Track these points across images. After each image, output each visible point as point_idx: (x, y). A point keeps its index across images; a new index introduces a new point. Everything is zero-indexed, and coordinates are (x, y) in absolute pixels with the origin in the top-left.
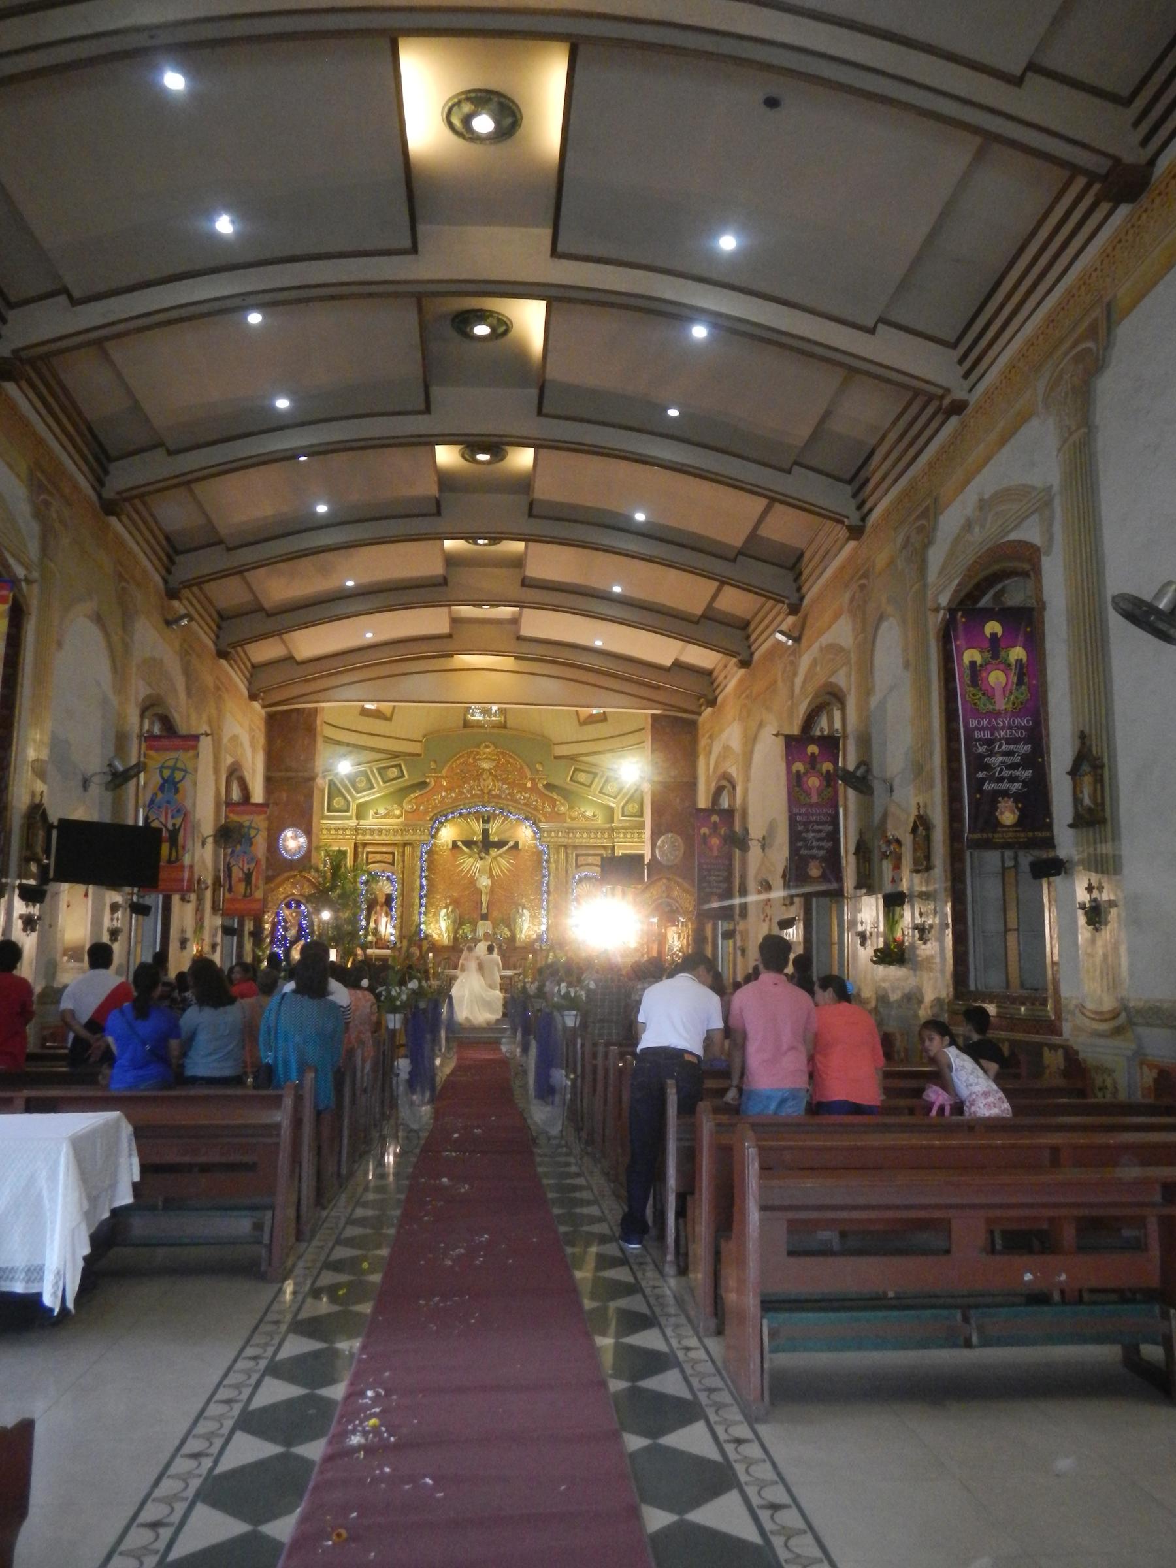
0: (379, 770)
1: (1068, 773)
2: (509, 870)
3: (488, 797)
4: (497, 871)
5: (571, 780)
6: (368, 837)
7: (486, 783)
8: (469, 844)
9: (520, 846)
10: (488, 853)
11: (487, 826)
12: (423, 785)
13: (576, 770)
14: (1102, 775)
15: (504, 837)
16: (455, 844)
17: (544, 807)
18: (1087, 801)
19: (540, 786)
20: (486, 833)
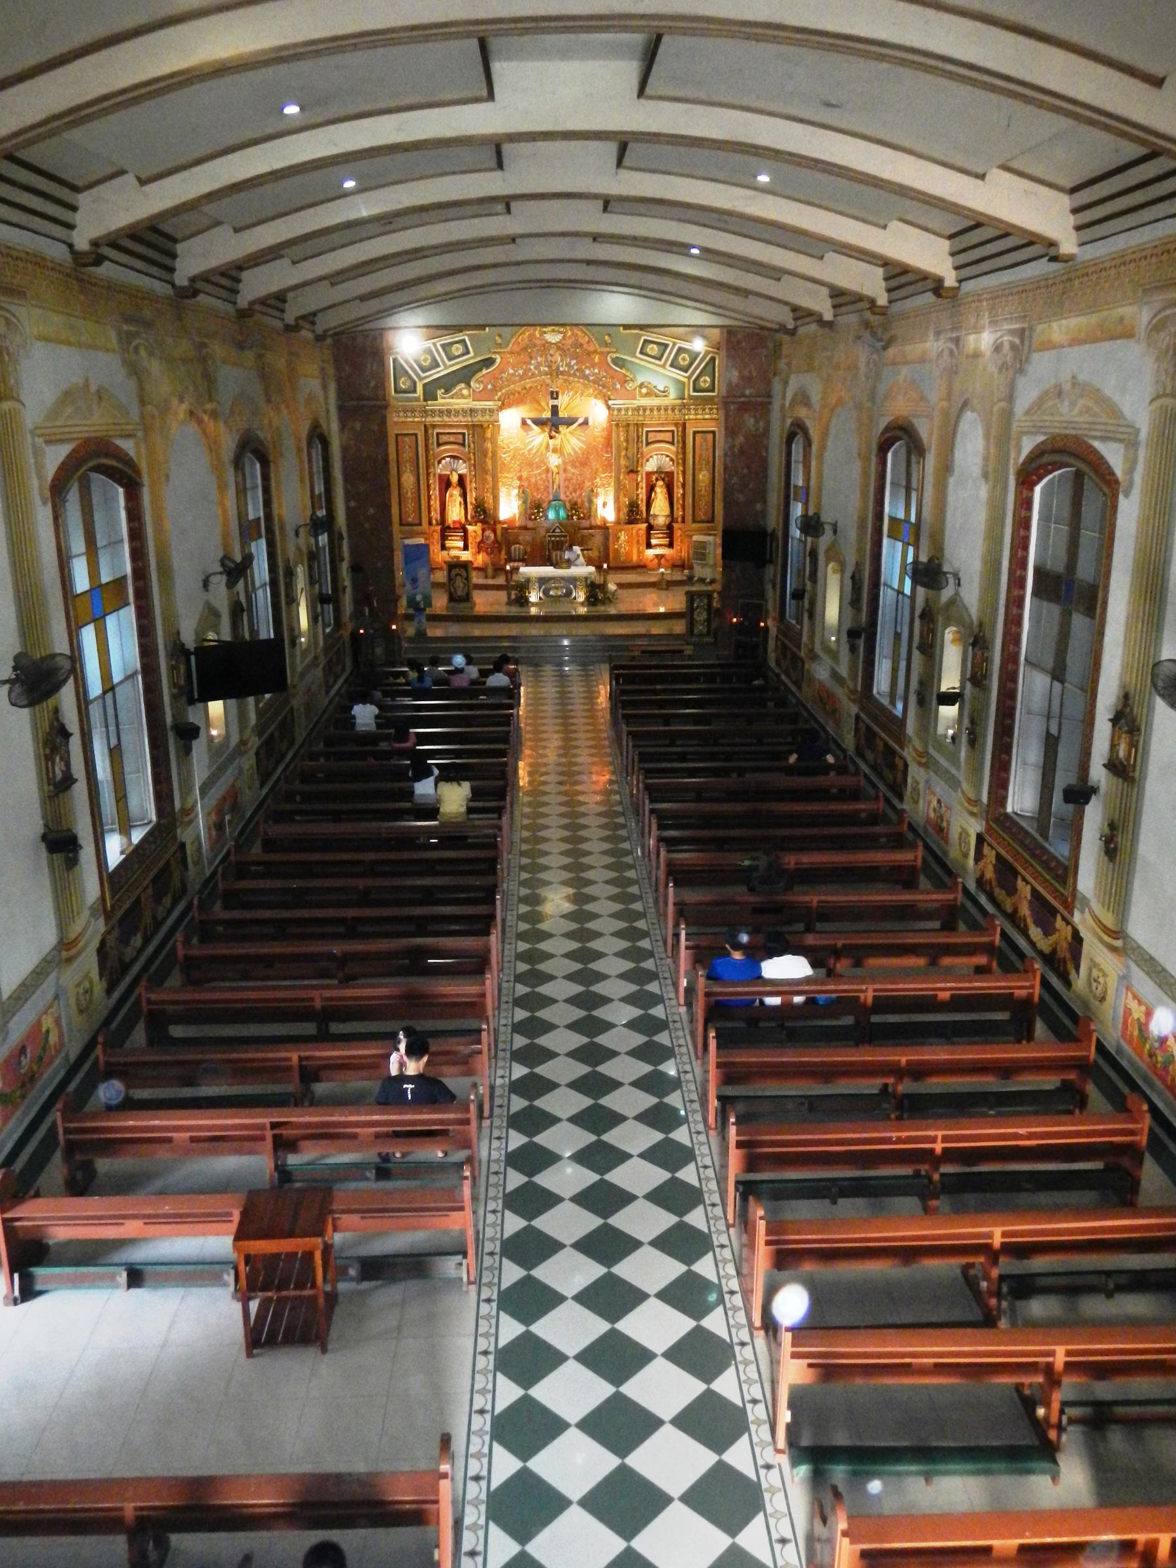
0: (443, 346)
1: (1110, 720)
2: (581, 448)
3: (555, 373)
4: (568, 449)
5: (641, 353)
6: (437, 419)
7: (553, 359)
8: (539, 422)
9: (590, 423)
10: (558, 432)
11: (555, 402)
12: (489, 362)
13: (646, 341)
14: (1138, 741)
15: (573, 414)
16: (524, 423)
17: (614, 384)
18: (1122, 754)
19: (609, 359)
20: (555, 410)
